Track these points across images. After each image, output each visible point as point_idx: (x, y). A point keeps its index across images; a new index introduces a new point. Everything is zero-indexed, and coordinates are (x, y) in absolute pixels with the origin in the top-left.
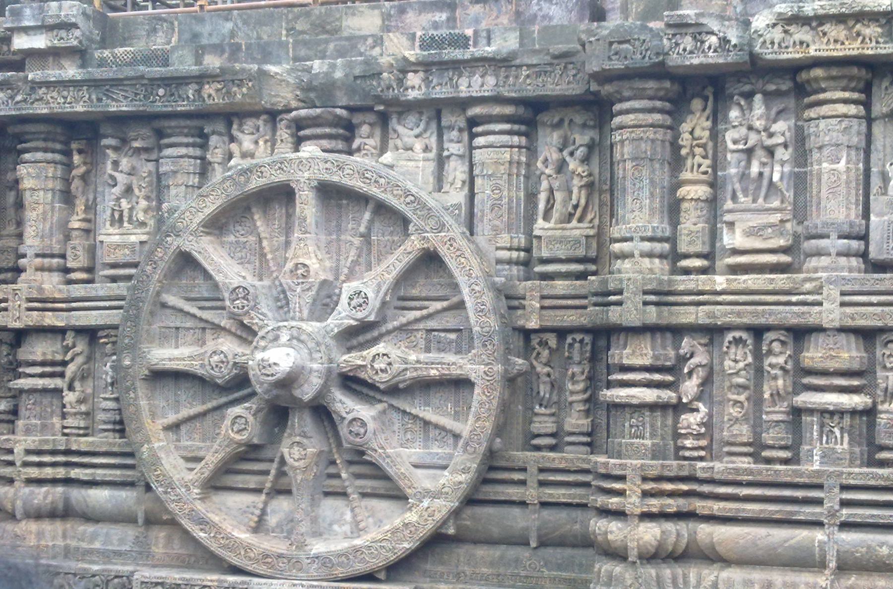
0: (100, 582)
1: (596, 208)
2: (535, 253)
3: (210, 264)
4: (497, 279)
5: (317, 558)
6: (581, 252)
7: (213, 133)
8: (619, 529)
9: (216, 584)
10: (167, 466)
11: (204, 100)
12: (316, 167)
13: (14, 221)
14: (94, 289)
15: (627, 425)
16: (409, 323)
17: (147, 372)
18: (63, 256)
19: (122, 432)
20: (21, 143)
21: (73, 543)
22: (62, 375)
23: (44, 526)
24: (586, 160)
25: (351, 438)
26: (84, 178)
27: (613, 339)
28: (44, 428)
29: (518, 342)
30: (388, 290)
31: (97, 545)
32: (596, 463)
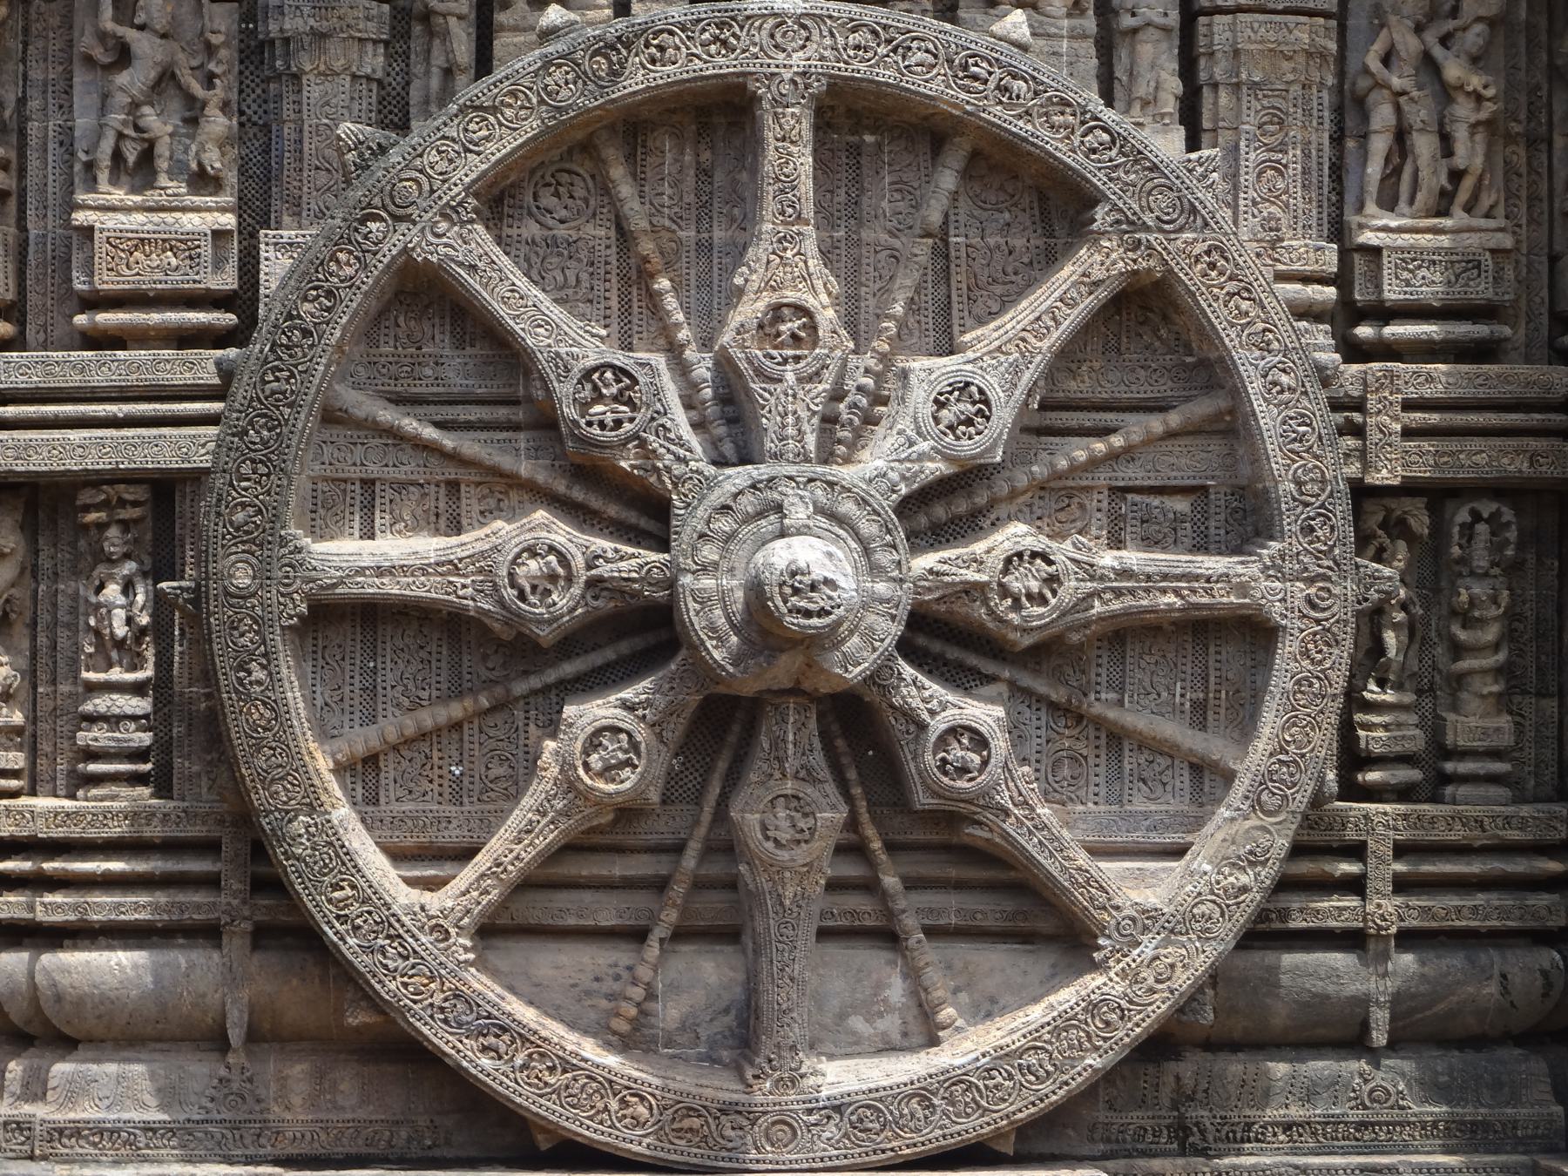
5: (838, 1109)
6: (1481, 290)
12: (828, 41)
16: (1075, 469)
17: (303, 608)
25: (945, 780)
31: (87, 1112)
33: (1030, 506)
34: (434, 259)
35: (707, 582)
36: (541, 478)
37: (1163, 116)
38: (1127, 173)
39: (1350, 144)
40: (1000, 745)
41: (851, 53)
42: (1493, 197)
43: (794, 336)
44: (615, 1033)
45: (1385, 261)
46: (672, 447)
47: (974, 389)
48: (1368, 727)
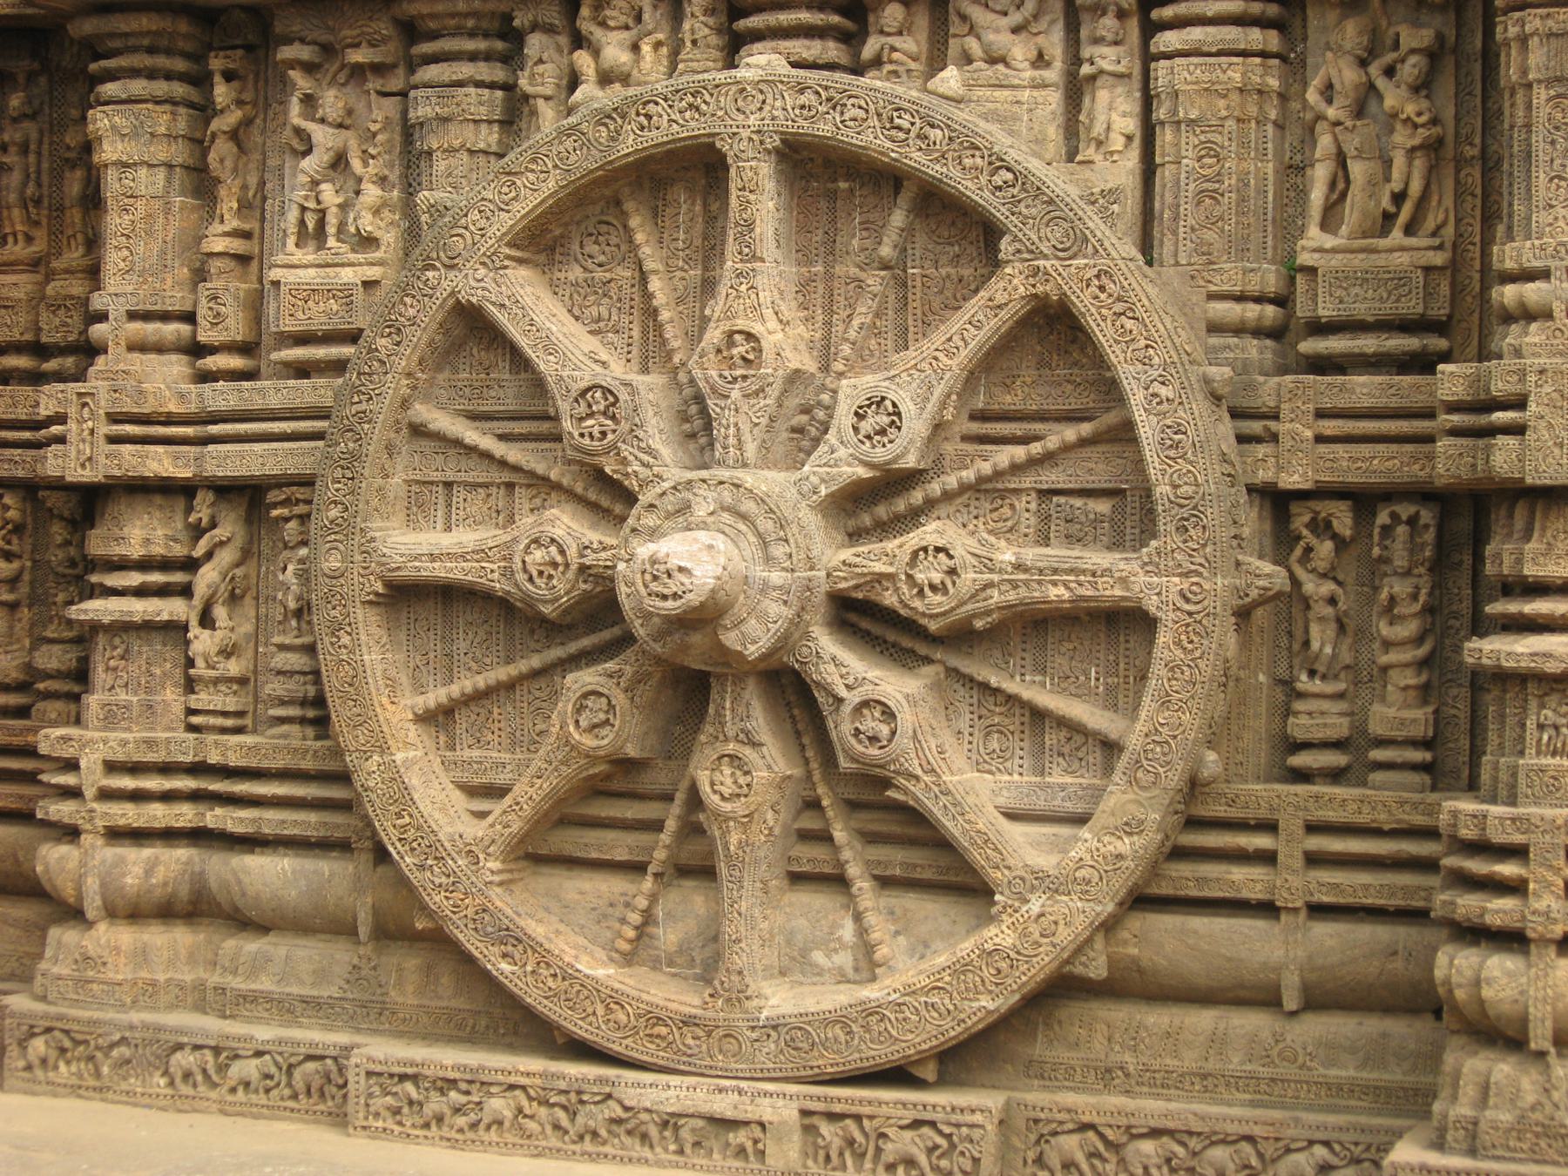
0: (273, 1070)
1: (1449, 201)
2: (1302, 310)
3: (526, 333)
4: (1216, 372)
5: (775, 1027)
6: (1412, 306)
7: (535, 27)
8: (1510, 975)
9: (538, 1081)
10: (425, 806)
12: (778, 104)
13: (80, 237)
14: (259, 391)
15: (1531, 724)
16: (998, 474)
17: (379, 587)
20: (98, 57)
21: (214, 979)
22: (186, 591)
23: (146, 937)
24: (1422, 87)
25: (860, 748)
26: (234, 135)
27: (1498, 518)
29: (1252, 520)
30: (948, 396)
31: (265, 984)
32: (1455, 814)
33: (968, 506)
34: (474, 300)
36: (565, 482)
37: (1112, 153)
38: (1027, 207)
39: (1309, 172)
41: (797, 111)
42: (1441, 217)
43: (744, 359)
44: (617, 951)
45: (1320, 280)
46: (641, 455)
47: (888, 403)
48: (1296, 714)
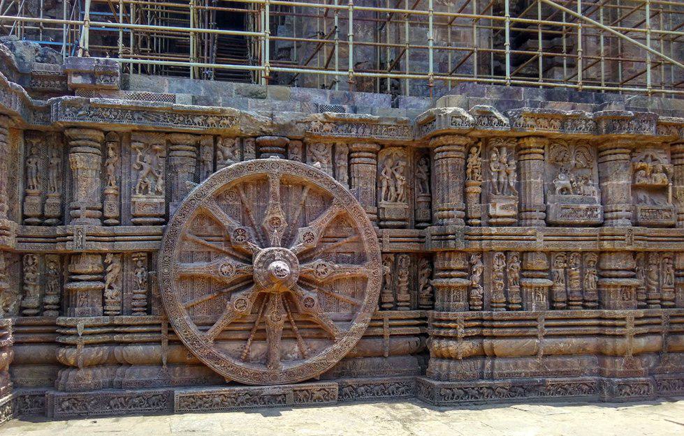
6: (403, 216)
11: (208, 126)
18: (102, 210)
19: (149, 312)
22: (103, 281)
28: (94, 313)
31: (134, 378)
35: (260, 270)
40: (316, 301)
